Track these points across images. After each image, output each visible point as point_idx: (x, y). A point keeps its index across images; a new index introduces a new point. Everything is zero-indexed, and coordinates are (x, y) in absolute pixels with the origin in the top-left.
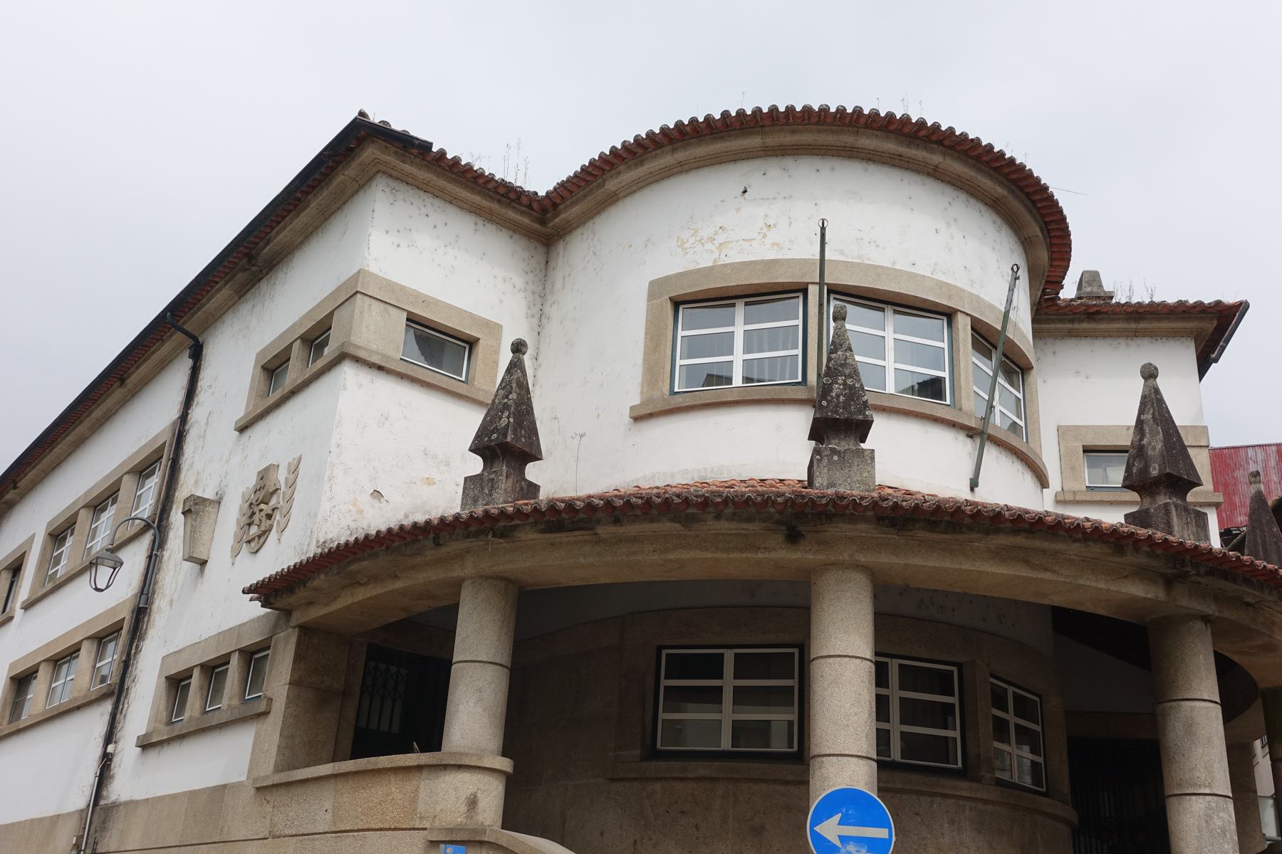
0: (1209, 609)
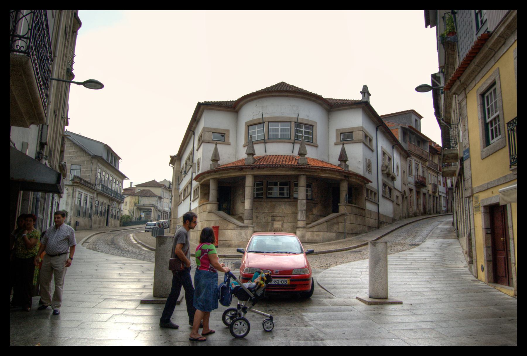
0: (304, 173)
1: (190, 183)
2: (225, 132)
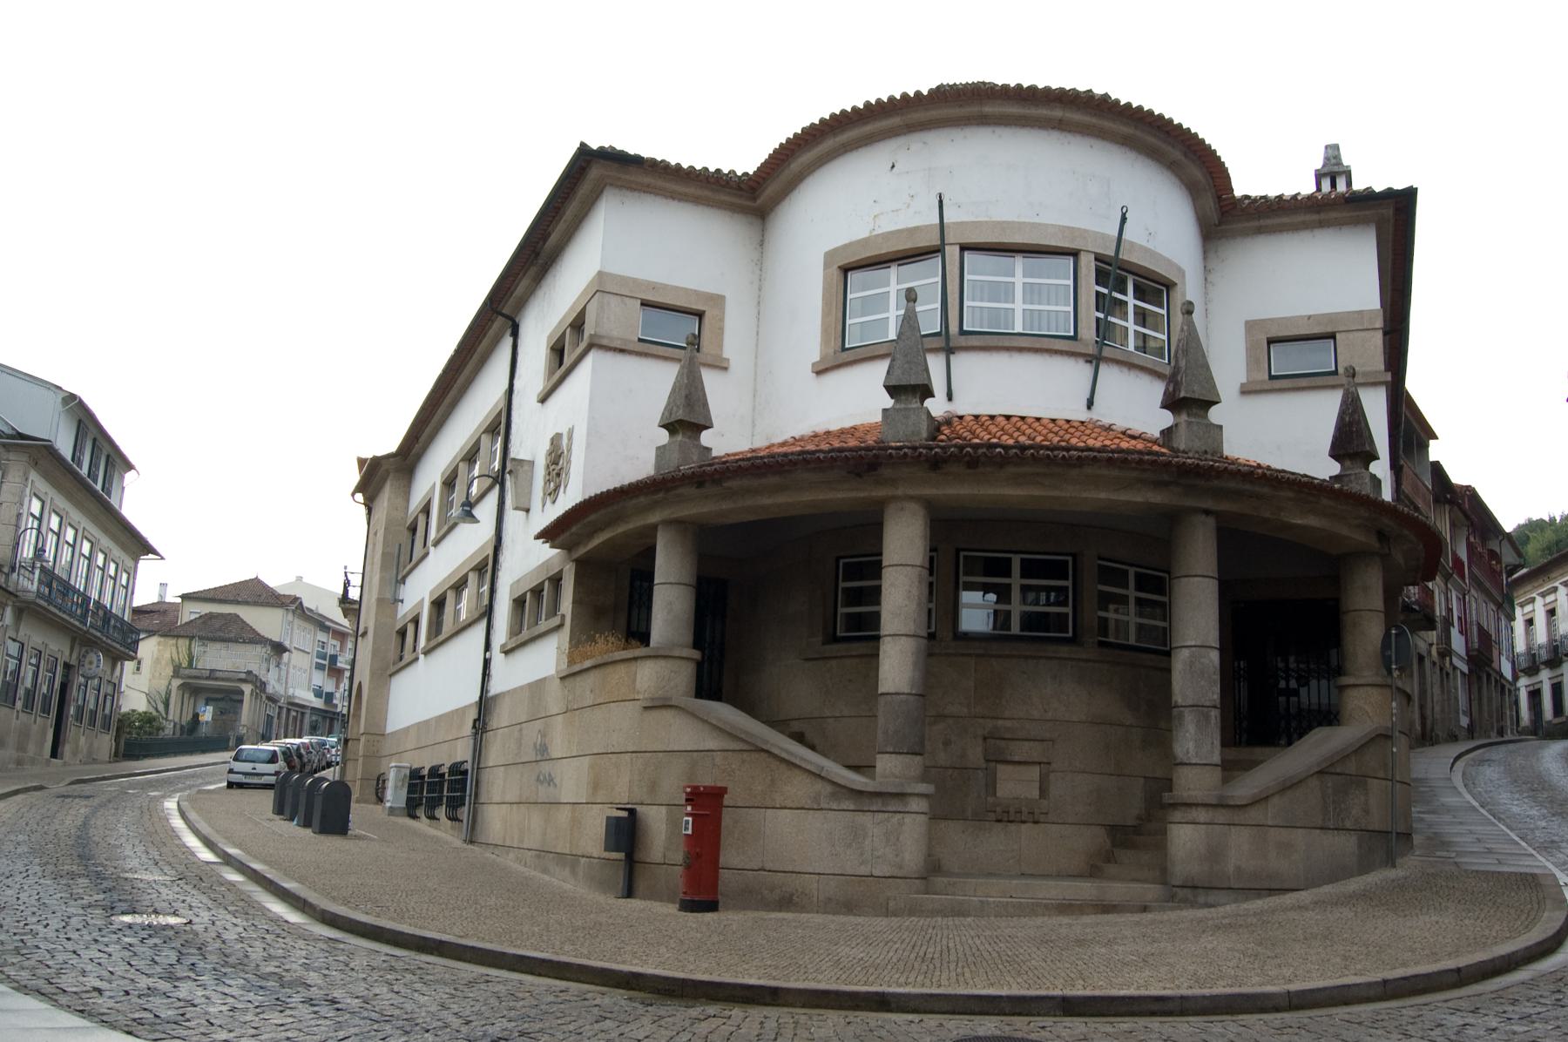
0: (1208, 504)
1: (480, 569)
2: (700, 307)
